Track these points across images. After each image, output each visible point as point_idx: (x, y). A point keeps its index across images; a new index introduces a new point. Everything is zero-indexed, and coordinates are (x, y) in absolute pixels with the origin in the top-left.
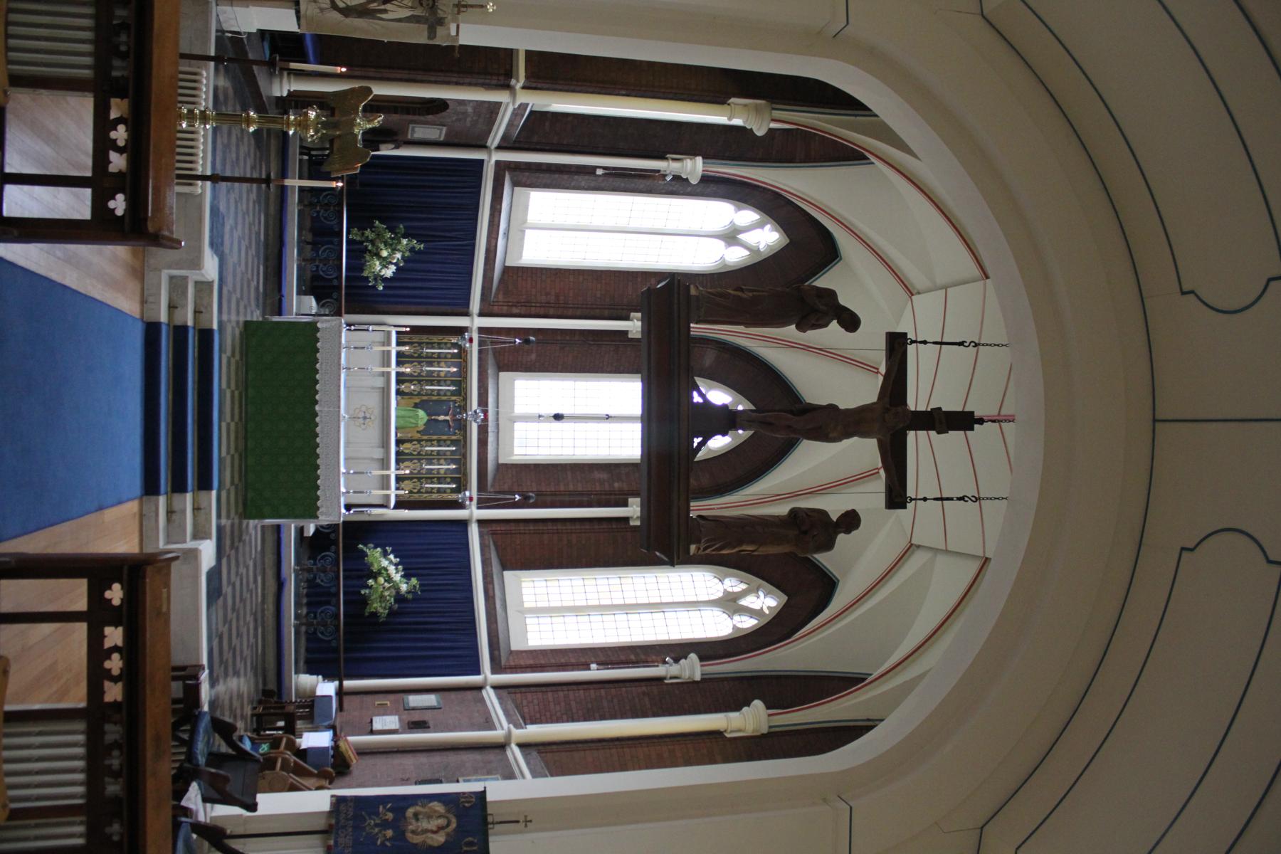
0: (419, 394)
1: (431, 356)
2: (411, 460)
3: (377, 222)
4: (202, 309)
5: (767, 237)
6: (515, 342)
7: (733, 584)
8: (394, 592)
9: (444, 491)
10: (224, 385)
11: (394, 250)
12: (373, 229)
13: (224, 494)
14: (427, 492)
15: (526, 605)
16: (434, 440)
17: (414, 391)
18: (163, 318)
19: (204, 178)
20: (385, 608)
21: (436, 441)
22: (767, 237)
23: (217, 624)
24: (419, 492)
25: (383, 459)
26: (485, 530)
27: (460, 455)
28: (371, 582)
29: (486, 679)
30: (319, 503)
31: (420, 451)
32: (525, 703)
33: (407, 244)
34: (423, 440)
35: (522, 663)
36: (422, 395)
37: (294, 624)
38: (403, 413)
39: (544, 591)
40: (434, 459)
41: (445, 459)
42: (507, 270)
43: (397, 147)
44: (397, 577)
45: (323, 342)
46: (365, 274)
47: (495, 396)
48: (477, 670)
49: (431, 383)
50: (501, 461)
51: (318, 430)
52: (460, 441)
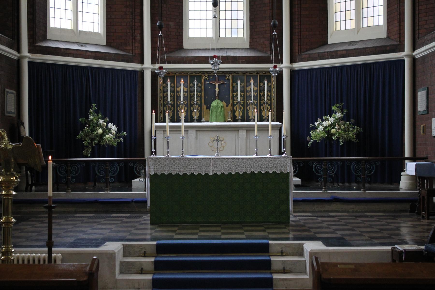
0: (200, 106)
1: (173, 97)
2: (247, 111)
3: (78, 137)
4: (143, 251)
6: (161, 36)
8: (341, 122)
9: (269, 87)
10: (196, 237)
11: (98, 125)
12: (83, 139)
13: (271, 236)
14: (270, 100)
15: (353, 27)
16: (233, 95)
17: (198, 109)
18: (149, 277)
19: (50, 253)
20: (354, 128)
21: (234, 93)
23: (363, 240)
24: (270, 105)
25: (247, 130)
26: (298, 57)
27: (244, 76)
28: (334, 138)
29: (407, 56)
30: (278, 172)
31: (241, 104)
32: (426, 26)
33: (93, 116)
34: (233, 103)
35: (396, 29)
36: (201, 103)
37: (363, 191)
38: (214, 118)
39: (343, 14)
40: (247, 95)
41: (247, 86)
42: (109, 44)
43: (23, 124)
44: (331, 120)
45: (165, 171)
46: (115, 144)
47: (201, 51)
48: (402, 62)
49: (192, 97)
50: (248, 47)
51: (226, 173)
52: (233, 76)
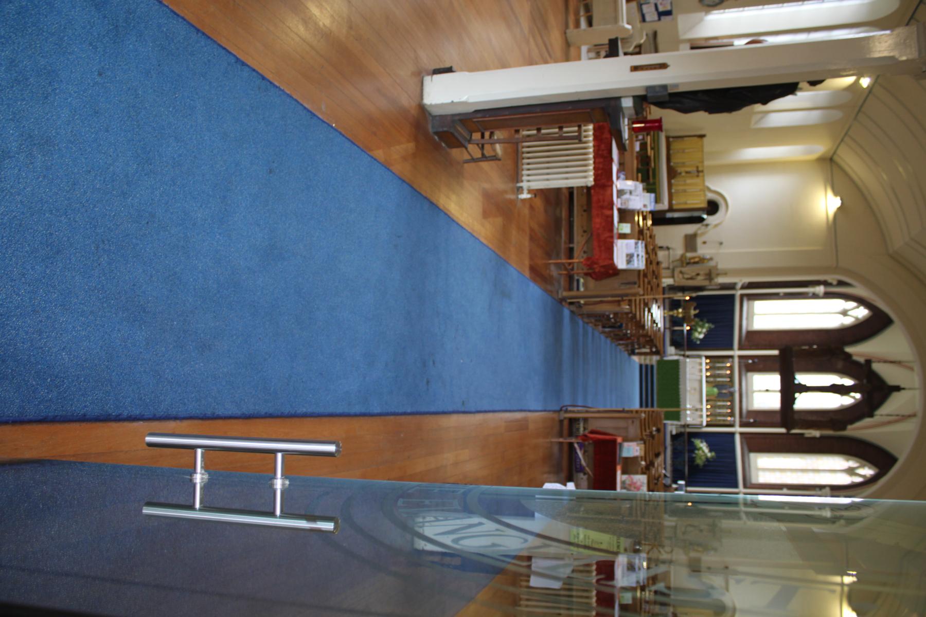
5: (862, 313)
7: (852, 464)
22: (862, 313)
